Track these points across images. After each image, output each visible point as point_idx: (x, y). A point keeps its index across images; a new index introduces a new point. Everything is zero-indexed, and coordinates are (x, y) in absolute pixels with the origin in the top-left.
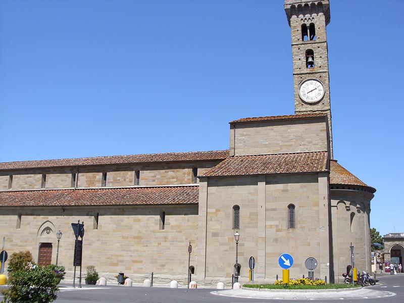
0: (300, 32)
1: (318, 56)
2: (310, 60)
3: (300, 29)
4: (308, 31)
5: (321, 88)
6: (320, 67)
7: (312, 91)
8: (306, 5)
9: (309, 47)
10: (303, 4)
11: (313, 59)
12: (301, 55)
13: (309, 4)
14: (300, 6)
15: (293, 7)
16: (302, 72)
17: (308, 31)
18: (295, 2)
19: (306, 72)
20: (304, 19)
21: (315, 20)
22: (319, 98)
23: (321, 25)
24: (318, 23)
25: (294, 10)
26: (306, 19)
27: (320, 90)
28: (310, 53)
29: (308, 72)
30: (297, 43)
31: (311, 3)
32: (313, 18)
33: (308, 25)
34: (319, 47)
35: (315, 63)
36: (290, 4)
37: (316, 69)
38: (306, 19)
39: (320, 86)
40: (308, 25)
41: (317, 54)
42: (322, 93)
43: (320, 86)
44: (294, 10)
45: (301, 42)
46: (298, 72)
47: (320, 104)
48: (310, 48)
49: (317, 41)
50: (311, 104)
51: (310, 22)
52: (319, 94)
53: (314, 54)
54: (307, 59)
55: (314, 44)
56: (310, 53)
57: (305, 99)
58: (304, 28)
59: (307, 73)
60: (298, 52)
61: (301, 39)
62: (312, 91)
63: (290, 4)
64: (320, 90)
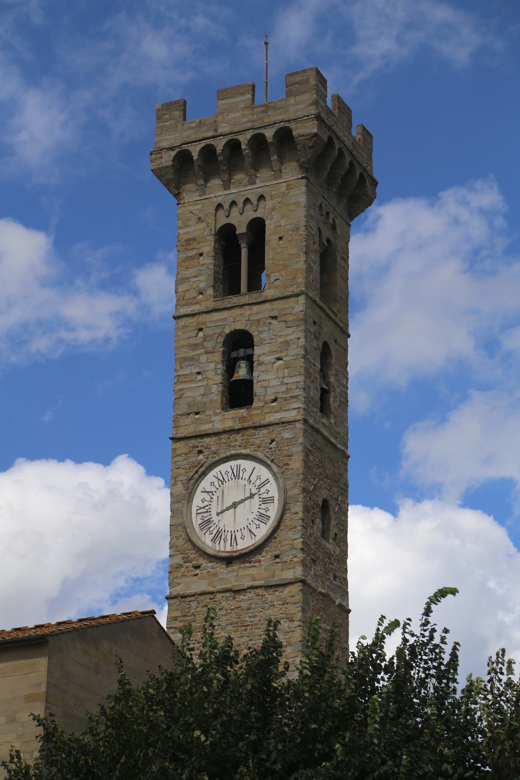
0: (208, 261)
1: (272, 358)
2: (242, 372)
3: (208, 247)
4: (244, 253)
5: (273, 489)
7: (235, 505)
8: (233, 146)
9: (235, 320)
10: (220, 145)
11: (251, 369)
12: (203, 358)
13: (244, 139)
14: (208, 151)
15: (183, 158)
16: (206, 428)
17: (244, 253)
18: (193, 138)
19: (219, 426)
20: (226, 206)
21: (269, 203)
22: (262, 532)
26: (233, 203)
27: (265, 501)
29: (229, 424)
30: (196, 308)
31: (249, 135)
32: (261, 197)
33: (241, 229)
34: (275, 318)
35: (257, 389)
36: (172, 149)
37: (259, 412)
38: (233, 203)
39: (267, 481)
40: (241, 229)
42: (273, 511)
43: (267, 481)
45: (211, 304)
47: (265, 557)
48: (239, 326)
49: (269, 293)
50: (229, 560)
51: (250, 214)
52: (263, 517)
53: (257, 351)
54: (230, 367)
55: (255, 308)
56: (239, 344)
57: (206, 541)
58: (226, 237)
59: (225, 432)
60: (195, 346)
61: (210, 291)
62: (235, 505)
63: (172, 149)
64: (265, 501)
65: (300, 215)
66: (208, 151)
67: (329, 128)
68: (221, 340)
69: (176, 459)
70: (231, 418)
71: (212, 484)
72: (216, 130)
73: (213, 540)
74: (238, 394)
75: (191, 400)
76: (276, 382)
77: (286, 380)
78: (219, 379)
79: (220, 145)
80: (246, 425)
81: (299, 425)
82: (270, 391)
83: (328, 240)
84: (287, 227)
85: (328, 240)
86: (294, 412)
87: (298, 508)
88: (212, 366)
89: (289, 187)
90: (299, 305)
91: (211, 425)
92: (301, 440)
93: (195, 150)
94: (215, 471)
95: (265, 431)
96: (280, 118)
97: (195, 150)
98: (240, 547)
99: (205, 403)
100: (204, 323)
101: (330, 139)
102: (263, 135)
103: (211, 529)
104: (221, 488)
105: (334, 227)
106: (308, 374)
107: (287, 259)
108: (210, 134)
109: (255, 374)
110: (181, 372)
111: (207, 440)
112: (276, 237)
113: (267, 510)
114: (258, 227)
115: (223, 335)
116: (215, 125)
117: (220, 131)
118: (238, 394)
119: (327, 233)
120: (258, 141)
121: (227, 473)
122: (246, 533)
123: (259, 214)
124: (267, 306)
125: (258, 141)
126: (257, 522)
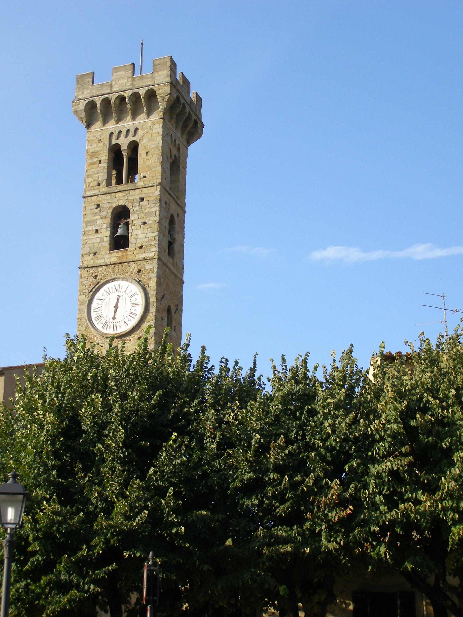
3: (104, 157)
6: (141, 247)
10: (113, 98)
14: (106, 102)
18: (98, 93)
19: (108, 261)
23: (152, 145)
24: (145, 141)
25: (96, 112)
27: (134, 305)
28: (121, 215)
30: (96, 192)
31: (130, 93)
37: (131, 253)
41: (136, 216)
44: (96, 112)
46: (91, 263)
48: (121, 203)
51: (131, 138)
53: (132, 217)
58: (115, 151)
63: (85, 99)
64: (134, 305)
65: (159, 140)
66: (106, 102)
67: (178, 91)
68: (111, 211)
69: (82, 280)
70: (115, 256)
71: (103, 295)
72: (111, 90)
73: (103, 327)
74: (119, 242)
75: (92, 245)
76: (143, 236)
77: (148, 235)
78: (108, 233)
79: (113, 98)
80: (123, 261)
81: (156, 261)
82: (139, 241)
83: (175, 156)
84: (152, 146)
85: (175, 156)
86: (153, 252)
87: (153, 309)
88: (105, 226)
89: (153, 123)
90: (157, 191)
91: (103, 260)
92: (156, 270)
93: (98, 101)
94: (105, 288)
95: (134, 265)
96: (149, 83)
97: (98, 101)
98: (118, 332)
99: (100, 248)
100: (100, 201)
101: (178, 98)
102: (138, 93)
103: (102, 321)
104: (108, 298)
105: (179, 149)
106: (160, 231)
107: (150, 165)
108: (108, 91)
109: (130, 231)
110: (87, 229)
111: (100, 269)
112: (145, 152)
113: (135, 310)
114: (134, 147)
115: (113, 208)
116: (111, 86)
117: (114, 90)
118: (119, 242)
119: (174, 152)
120: (136, 97)
121: (112, 288)
122: (122, 323)
123: (135, 139)
124: (137, 191)
125: (136, 97)
126: (130, 317)
